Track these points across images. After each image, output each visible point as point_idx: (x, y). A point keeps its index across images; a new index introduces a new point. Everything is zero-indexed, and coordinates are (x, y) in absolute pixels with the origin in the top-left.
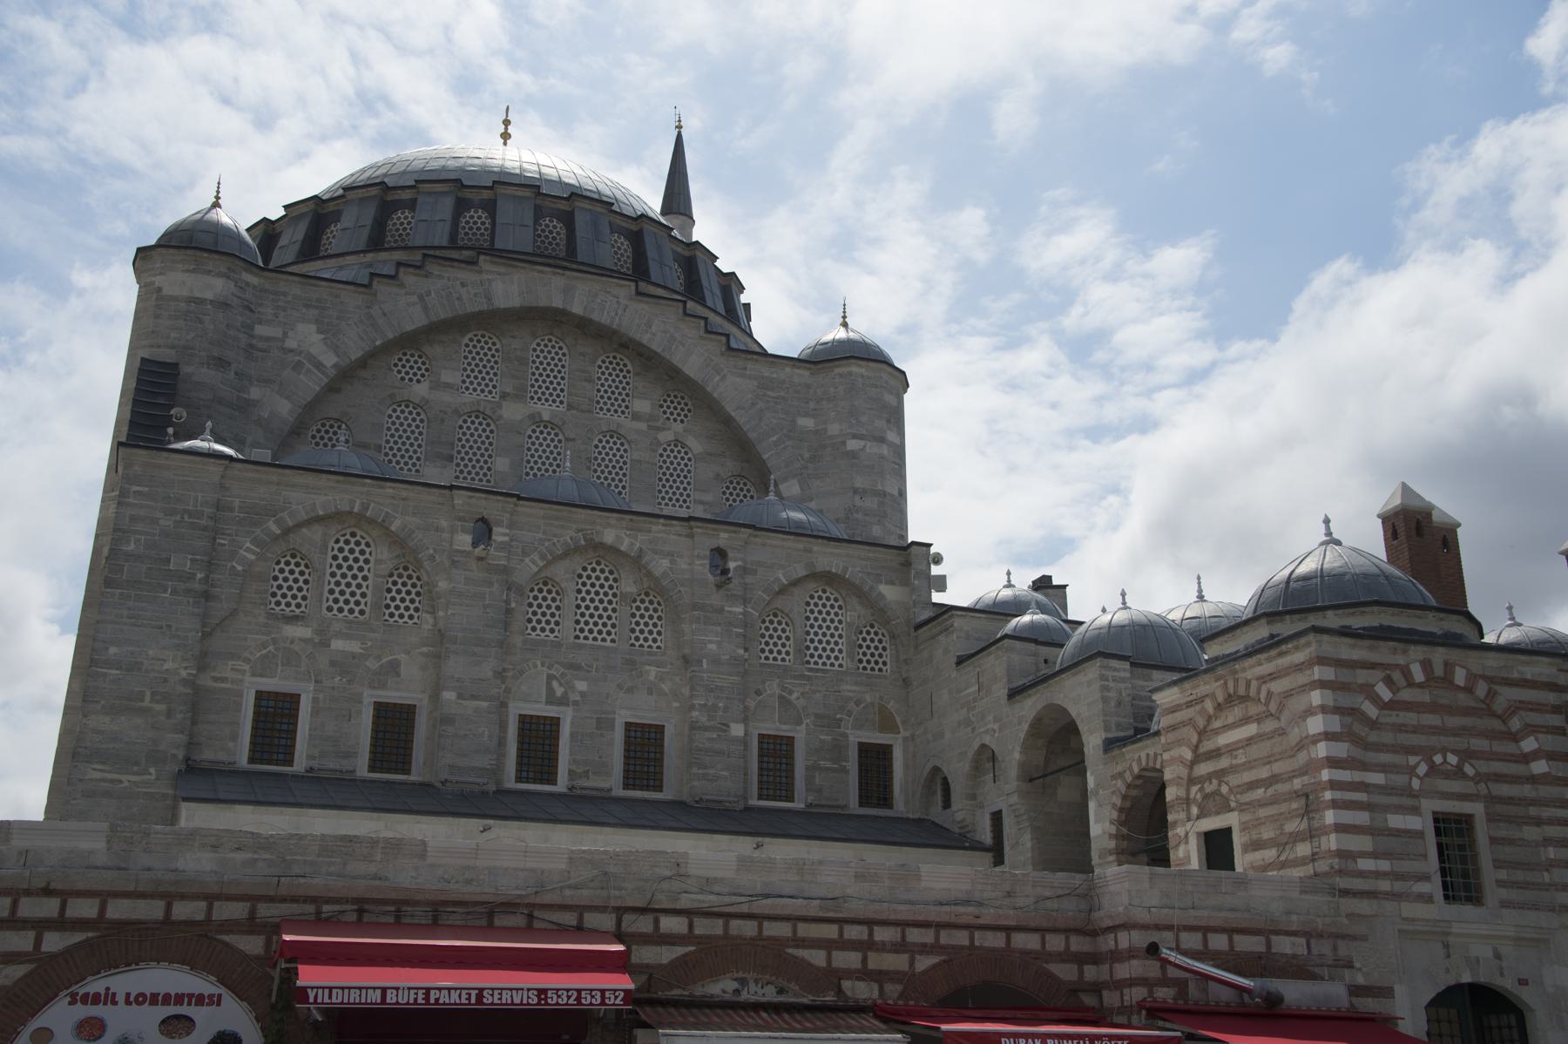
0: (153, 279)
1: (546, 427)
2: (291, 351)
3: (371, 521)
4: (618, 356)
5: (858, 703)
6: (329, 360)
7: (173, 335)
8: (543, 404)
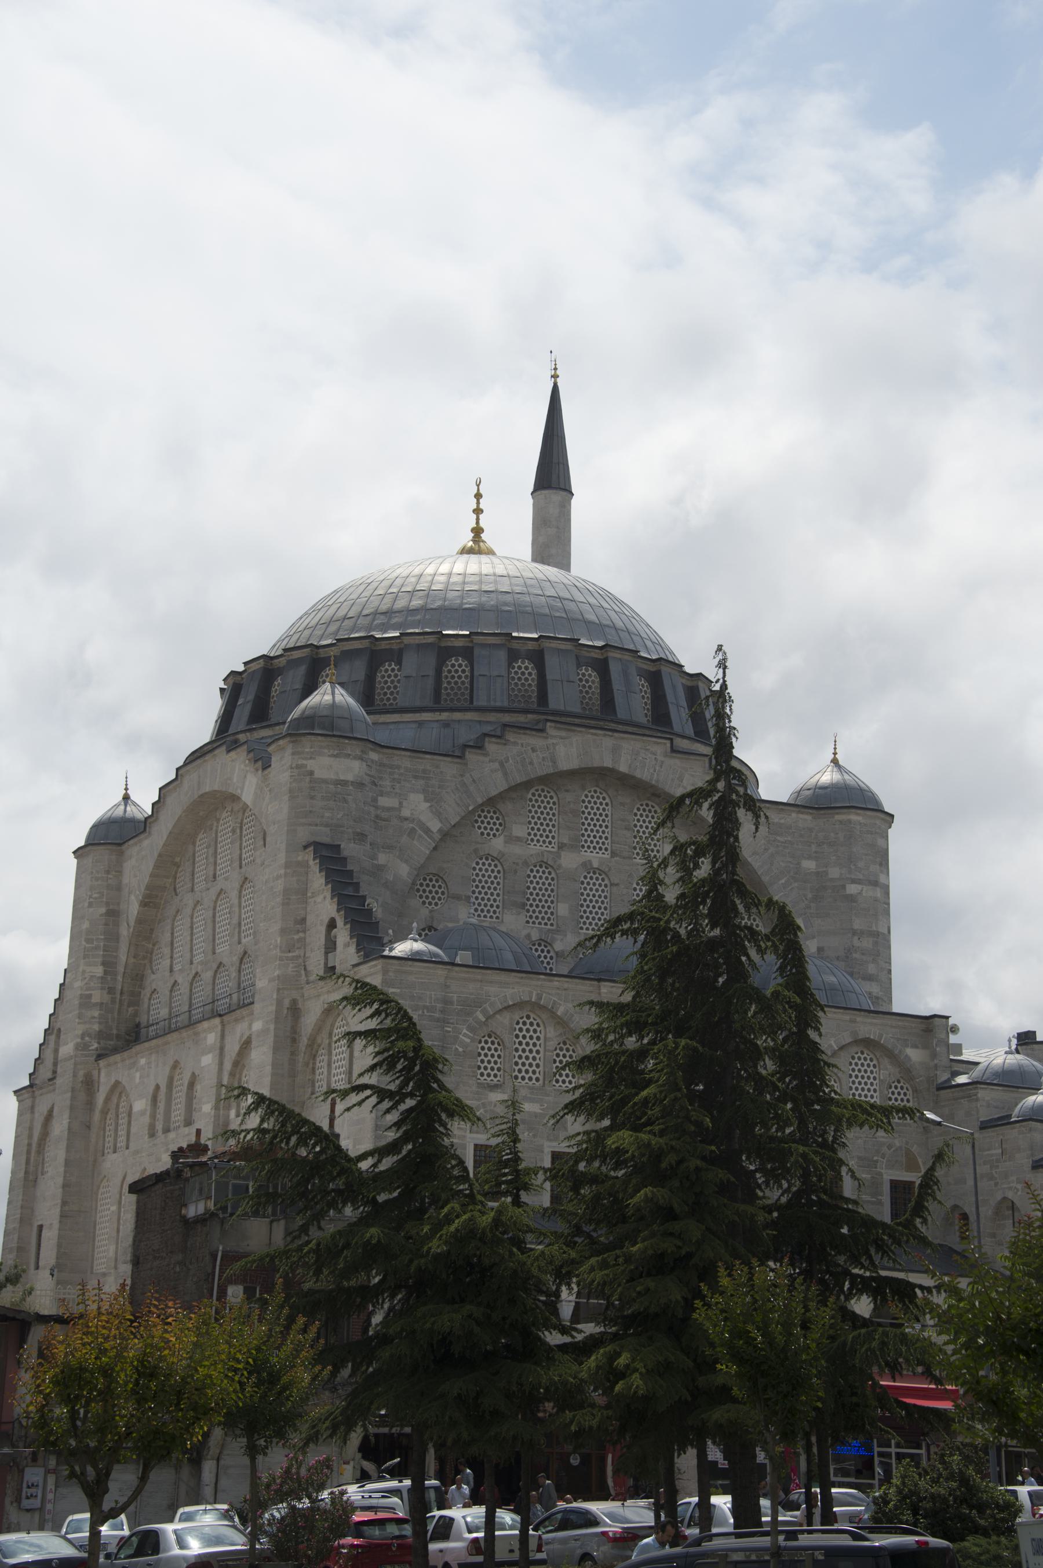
0: (305, 762)
1: (594, 873)
2: (406, 819)
3: (543, 1008)
4: (650, 803)
5: (889, 1147)
6: (435, 825)
7: (327, 814)
8: (591, 852)
